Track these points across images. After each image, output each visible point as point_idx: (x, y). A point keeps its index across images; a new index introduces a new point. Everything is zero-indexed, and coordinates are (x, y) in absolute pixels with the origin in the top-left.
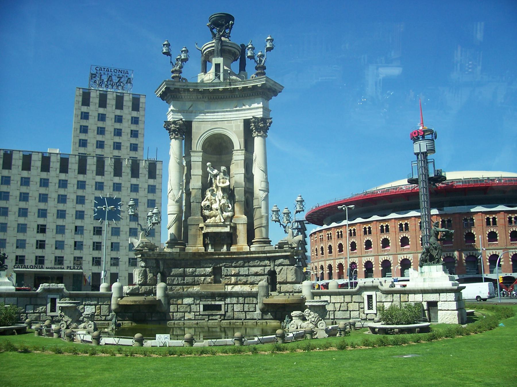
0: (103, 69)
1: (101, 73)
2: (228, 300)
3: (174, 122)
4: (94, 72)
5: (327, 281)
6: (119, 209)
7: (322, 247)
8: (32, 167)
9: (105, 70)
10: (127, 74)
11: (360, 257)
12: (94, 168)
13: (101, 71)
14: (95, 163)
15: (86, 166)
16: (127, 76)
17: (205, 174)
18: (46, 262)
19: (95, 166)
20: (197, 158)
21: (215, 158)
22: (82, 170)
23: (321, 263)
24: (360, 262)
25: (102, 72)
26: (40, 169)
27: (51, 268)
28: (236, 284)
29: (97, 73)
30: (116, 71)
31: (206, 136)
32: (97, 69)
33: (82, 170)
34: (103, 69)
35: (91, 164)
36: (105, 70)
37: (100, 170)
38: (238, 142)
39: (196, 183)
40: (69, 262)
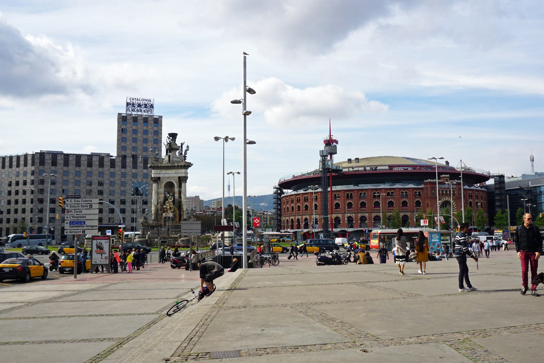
0: (134, 99)
1: (133, 102)
2: (169, 239)
3: (154, 178)
4: (129, 101)
5: (296, 230)
6: (147, 188)
7: (288, 207)
8: (93, 165)
9: (136, 99)
10: (150, 102)
11: (302, 215)
12: (131, 164)
13: (133, 101)
14: (132, 162)
15: (126, 163)
16: (150, 103)
17: (165, 196)
18: (103, 221)
19: (132, 163)
20: (162, 190)
21: (169, 189)
22: (124, 166)
23: (291, 218)
24: (302, 218)
25: (134, 101)
26: (98, 166)
27: (107, 224)
28: (174, 234)
29: (131, 102)
30: (143, 100)
31: (167, 181)
32: (131, 99)
33: (124, 166)
34: (134, 99)
35: (129, 160)
36: (136, 99)
37: (135, 166)
38: (176, 185)
39: (162, 200)
40: (117, 221)
